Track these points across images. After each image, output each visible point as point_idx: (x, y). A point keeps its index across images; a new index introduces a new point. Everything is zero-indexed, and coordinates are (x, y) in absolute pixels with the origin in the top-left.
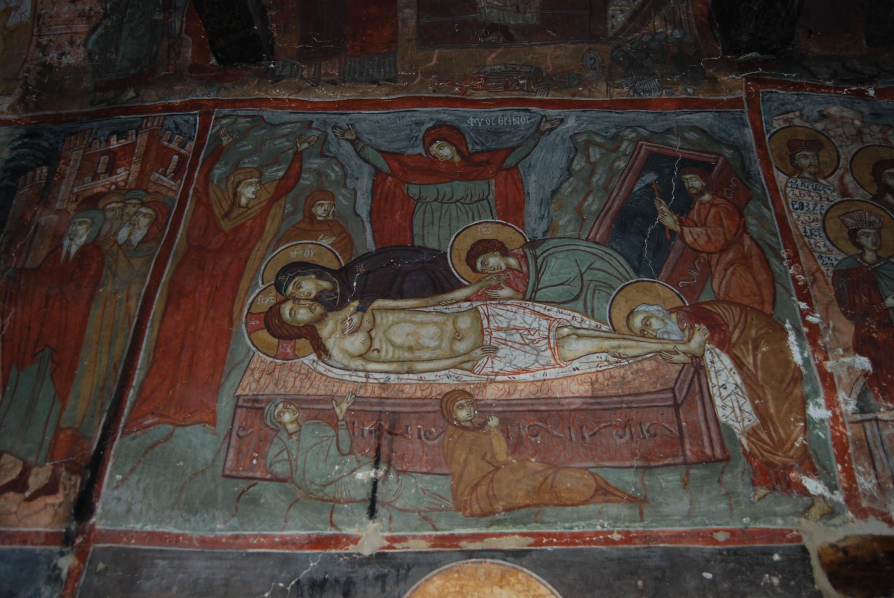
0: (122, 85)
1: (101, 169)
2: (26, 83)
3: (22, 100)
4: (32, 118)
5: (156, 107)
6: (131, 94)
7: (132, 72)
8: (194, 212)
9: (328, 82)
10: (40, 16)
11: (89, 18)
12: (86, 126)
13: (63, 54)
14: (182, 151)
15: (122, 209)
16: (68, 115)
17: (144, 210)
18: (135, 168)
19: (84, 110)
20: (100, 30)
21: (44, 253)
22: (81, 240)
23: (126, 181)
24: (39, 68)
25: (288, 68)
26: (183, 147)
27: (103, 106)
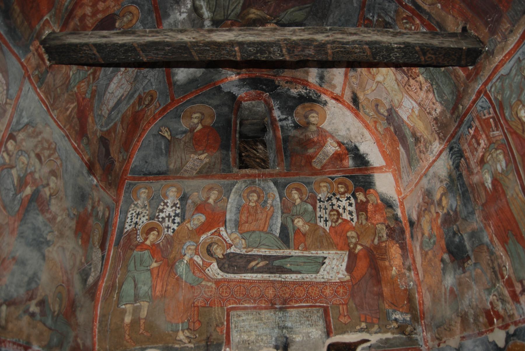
0: (455, 108)
1: (476, 146)
2: (436, 131)
3: (440, 138)
4: (447, 142)
5: (470, 105)
6: (461, 107)
7: (455, 98)
8: (513, 139)
9: (509, 33)
10: (419, 103)
11: (429, 90)
12: (460, 132)
13: (435, 110)
14: (491, 115)
15: (492, 157)
16: (453, 132)
17: (498, 152)
18: (484, 136)
19: (456, 126)
20: (435, 91)
21: (484, 193)
22: (489, 181)
23: (485, 144)
24: (435, 122)
25: (492, 44)
26: (490, 114)
27: (458, 120)
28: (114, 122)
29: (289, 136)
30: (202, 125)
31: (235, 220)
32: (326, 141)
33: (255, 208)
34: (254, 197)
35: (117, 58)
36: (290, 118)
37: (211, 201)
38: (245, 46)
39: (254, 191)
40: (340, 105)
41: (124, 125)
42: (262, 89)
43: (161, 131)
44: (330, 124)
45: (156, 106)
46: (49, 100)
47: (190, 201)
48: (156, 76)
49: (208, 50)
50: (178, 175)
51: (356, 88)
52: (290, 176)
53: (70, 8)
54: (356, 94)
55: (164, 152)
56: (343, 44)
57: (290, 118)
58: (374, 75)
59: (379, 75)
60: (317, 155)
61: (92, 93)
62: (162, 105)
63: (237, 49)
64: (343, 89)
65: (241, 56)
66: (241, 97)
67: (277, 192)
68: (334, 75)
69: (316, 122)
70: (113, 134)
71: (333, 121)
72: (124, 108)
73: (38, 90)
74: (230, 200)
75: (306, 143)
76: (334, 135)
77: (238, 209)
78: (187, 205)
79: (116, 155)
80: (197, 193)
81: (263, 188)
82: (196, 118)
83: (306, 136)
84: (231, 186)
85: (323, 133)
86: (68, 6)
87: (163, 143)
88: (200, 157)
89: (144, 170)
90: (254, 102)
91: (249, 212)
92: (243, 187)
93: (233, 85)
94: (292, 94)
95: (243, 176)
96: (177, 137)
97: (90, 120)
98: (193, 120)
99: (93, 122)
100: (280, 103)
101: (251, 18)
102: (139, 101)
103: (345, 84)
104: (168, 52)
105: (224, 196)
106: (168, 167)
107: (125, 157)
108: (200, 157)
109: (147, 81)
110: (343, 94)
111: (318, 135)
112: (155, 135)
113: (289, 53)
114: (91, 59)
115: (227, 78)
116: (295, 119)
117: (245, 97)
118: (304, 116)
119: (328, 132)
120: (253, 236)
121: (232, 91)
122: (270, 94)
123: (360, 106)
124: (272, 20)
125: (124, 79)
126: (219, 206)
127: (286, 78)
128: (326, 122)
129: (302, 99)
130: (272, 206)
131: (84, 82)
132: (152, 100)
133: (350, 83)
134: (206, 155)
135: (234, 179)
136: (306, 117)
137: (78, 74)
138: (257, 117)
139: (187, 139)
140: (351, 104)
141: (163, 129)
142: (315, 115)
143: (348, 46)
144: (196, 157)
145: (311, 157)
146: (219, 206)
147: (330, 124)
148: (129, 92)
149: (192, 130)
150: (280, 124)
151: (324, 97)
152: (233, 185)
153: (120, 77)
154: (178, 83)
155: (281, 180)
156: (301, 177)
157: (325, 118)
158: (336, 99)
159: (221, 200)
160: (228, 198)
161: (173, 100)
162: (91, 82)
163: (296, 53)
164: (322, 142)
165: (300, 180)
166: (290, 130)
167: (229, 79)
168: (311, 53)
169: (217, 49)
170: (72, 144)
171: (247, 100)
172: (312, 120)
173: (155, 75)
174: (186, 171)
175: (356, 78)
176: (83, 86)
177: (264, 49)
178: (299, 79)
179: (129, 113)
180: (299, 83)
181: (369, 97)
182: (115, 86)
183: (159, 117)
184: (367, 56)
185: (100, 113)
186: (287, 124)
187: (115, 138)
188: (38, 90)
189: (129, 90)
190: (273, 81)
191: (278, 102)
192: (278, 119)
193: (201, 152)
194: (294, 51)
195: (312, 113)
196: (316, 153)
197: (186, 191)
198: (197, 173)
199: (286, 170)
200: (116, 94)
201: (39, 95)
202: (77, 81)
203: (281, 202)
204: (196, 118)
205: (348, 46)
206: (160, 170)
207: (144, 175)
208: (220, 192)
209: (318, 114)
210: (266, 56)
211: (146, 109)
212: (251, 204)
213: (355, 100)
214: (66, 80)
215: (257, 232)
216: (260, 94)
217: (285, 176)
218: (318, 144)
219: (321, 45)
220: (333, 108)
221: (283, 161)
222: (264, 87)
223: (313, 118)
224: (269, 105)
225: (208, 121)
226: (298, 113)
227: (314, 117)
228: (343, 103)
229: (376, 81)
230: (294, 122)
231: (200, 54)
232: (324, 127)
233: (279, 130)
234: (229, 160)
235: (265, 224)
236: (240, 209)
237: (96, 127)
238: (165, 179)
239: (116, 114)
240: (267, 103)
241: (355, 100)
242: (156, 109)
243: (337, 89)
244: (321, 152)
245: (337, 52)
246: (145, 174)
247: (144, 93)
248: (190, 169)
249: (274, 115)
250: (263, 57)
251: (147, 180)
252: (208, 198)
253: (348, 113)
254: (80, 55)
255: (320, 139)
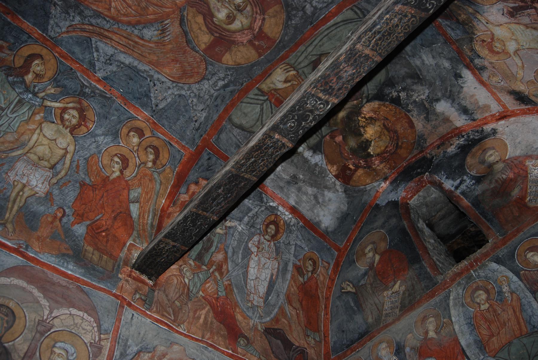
28: (278, 307)
29: (477, 197)
30: (379, 254)
31: (475, 341)
32: (527, 167)
33: (490, 309)
34: (482, 296)
35: (194, 235)
36: (465, 177)
37: (432, 334)
38: (281, 126)
39: (478, 288)
40: (512, 119)
41: (294, 305)
42: (418, 174)
43: (343, 288)
44: (516, 147)
45: (325, 267)
46: (166, 316)
47: (407, 350)
48: (300, 237)
49: (255, 161)
50: (382, 325)
51: (506, 85)
52: (510, 239)
53: (156, 223)
54: (513, 90)
55: (356, 309)
56: (371, 31)
57: (465, 177)
58: (503, 51)
59: (508, 44)
60: (526, 190)
61: (226, 289)
62: (331, 261)
63: (277, 136)
64: (499, 100)
65: (289, 140)
66: (403, 198)
67: (507, 270)
68: (473, 96)
69: (498, 159)
70: (283, 320)
71: (517, 141)
72: (284, 286)
73: (148, 312)
74: (453, 319)
75: (503, 189)
76: (530, 153)
77: (469, 324)
78: (407, 356)
79: (302, 342)
80: (411, 335)
81: (486, 277)
82: (369, 252)
83: (496, 181)
84: (446, 301)
85: (515, 161)
86: (152, 223)
87: (351, 300)
88: (394, 290)
89: (345, 341)
90: (421, 193)
91: (486, 320)
92: (461, 291)
93: (388, 193)
94: (451, 154)
95: (453, 280)
96: (361, 284)
97: (239, 317)
98: (368, 256)
99: (244, 319)
100: (445, 172)
101: (343, 118)
102: (298, 272)
103: (493, 94)
104: (226, 194)
105: (444, 318)
106: (367, 323)
107: (318, 339)
108: (394, 290)
109: (293, 247)
110: (504, 106)
111: (511, 169)
112: (339, 296)
113: (330, 94)
114: (176, 252)
115: (378, 192)
116: (472, 173)
117: (407, 195)
118: (480, 163)
119: (520, 157)
120: (513, 349)
121: (390, 200)
122: (429, 172)
123: (533, 99)
124: (362, 102)
125: (262, 259)
126: (444, 334)
127: (435, 144)
128: (509, 148)
129: (465, 150)
130: (512, 293)
131: (209, 282)
132: (315, 263)
133: (495, 87)
134: (399, 281)
135: (445, 289)
136: (483, 162)
137: (196, 278)
138: (439, 206)
139: (371, 278)
140: (523, 107)
141: (344, 285)
142: (491, 152)
143: (379, 27)
144: (390, 292)
145: (522, 199)
146: (444, 334)
147: (516, 147)
148: (278, 268)
149: (371, 266)
150: (458, 192)
151: (488, 128)
152: (448, 297)
153: (256, 259)
154: (330, 230)
155: (502, 252)
156: (525, 230)
157: (506, 145)
158: (503, 116)
159: (443, 326)
160: (450, 317)
161: (339, 250)
162: (219, 278)
163: (337, 87)
164: (521, 172)
165: (528, 235)
166: (474, 189)
167: (381, 190)
168: (350, 72)
169: (261, 153)
170: (223, 352)
171: (412, 197)
172: (492, 159)
173: (297, 237)
174: (387, 315)
175: (494, 75)
176: (209, 287)
177: (301, 112)
178: (448, 134)
179: (294, 289)
180: (452, 137)
181: (527, 78)
182: (256, 270)
183: (336, 276)
184: (413, 16)
185: (250, 305)
186: (466, 186)
187: (289, 323)
188: (148, 312)
189: (277, 266)
190: (424, 158)
191: (443, 173)
192: (453, 189)
193: (393, 283)
194: (331, 87)
195: (487, 153)
196: (524, 191)
197: (398, 339)
198: (400, 310)
199: (500, 235)
200: (263, 277)
201: (150, 317)
202: (199, 285)
203: (521, 280)
204: (369, 252)
205: (379, 27)
206: (360, 331)
207: (347, 347)
208: (437, 316)
209: (493, 148)
210: (311, 118)
211: (315, 275)
212: (483, 307)
213: (520, 97)
214: (184, 289)
215: (515, 341)
216: (419, 180)
217: (504, 244)
218: (519, 179)
219: (351, 54)
220: (506, 129)
221: (489, 228)
222: (419, 170)
223: (492, 157)
224: (436, 182)
225: (383, 246)
226: (470, 166)
227: (491, 155)
228: (513, 114)
229: (512, 54)
230: (473, 178)
231: (253, 171)
232: (513, 155)
233: (462, 199)
234: (426, 272)
235: (519, 323)
236: (473, 324)
237: (251, 321)
238: (371, 339)
239: (275, 297)
240: (434, 183)
241: (520, 97)
242: (327, 270)
243: (492, 106)
244: (529, 184)
245: (377, 44)
246: (348, 346)
247: (299, 261)
248: (390, 311)
249: (447, 188)
250: (311, 122)
251: (352, 352)
252: (427, 333)
253: (528, 119)
254: (165, 256)
255: (516, 171)
